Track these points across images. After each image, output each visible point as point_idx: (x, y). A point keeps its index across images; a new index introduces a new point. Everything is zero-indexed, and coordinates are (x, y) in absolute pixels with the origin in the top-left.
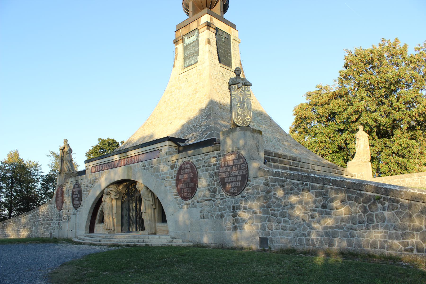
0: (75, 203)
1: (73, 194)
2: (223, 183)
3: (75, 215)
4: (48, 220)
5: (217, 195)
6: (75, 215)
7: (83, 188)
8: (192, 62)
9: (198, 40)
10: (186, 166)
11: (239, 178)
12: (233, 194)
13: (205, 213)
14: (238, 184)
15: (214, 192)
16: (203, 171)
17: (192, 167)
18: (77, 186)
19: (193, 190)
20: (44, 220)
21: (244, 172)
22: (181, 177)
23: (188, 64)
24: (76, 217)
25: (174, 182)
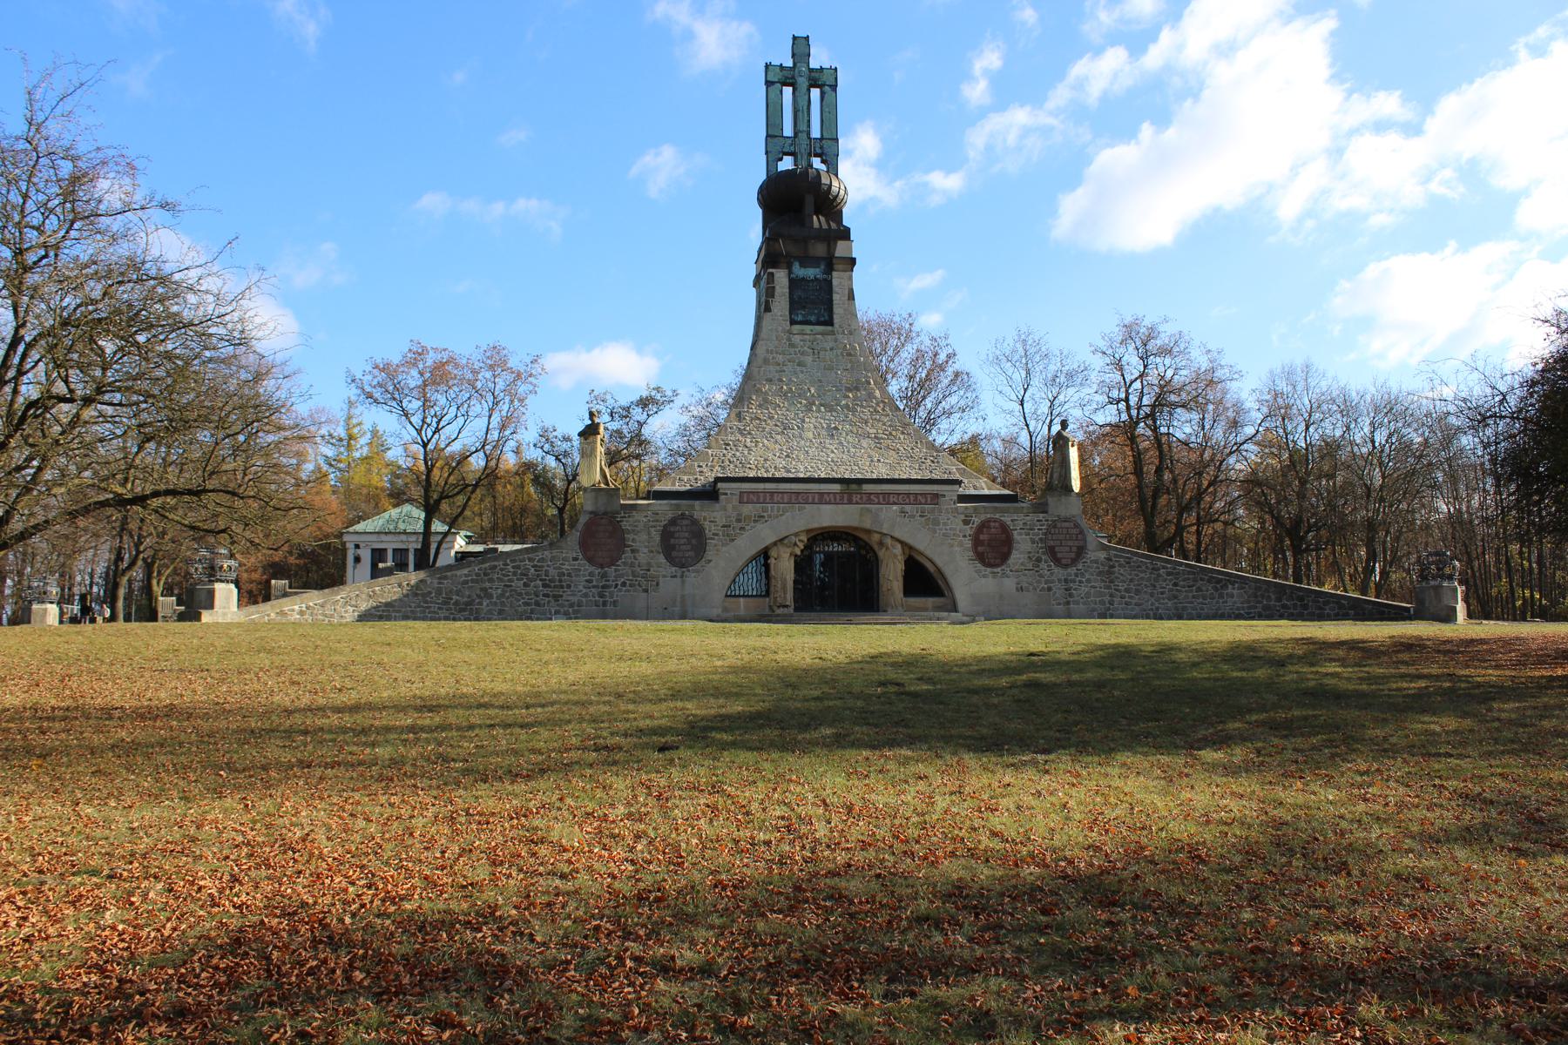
0: (674, 554)
1: (667, 535)
2: (1052, 552)
3: (678, 580)
4: (545, 586)
5: (1043, 565)
6: (678, 580)
7: (709, 529)
8: (813, 318)
9: (830, 283)
10: (992, 524)
11: (1074, 549)
12: (1066, 566)
13: (1025, 585)
14: (1073, 555)
15: (1039, 560)
16: (1020, 534)
17: (1004, 528)
18: (685, 522)
19: (1004, 557)
20: (525, 585)
21: (1081, 543)
22: (982, 537)
23: (800, 318)
24: (683, 582)
25: (968, 543)
